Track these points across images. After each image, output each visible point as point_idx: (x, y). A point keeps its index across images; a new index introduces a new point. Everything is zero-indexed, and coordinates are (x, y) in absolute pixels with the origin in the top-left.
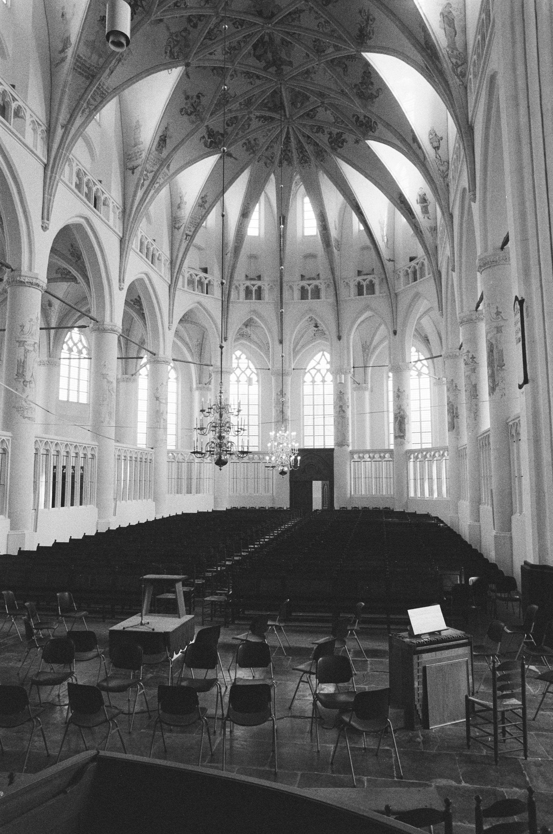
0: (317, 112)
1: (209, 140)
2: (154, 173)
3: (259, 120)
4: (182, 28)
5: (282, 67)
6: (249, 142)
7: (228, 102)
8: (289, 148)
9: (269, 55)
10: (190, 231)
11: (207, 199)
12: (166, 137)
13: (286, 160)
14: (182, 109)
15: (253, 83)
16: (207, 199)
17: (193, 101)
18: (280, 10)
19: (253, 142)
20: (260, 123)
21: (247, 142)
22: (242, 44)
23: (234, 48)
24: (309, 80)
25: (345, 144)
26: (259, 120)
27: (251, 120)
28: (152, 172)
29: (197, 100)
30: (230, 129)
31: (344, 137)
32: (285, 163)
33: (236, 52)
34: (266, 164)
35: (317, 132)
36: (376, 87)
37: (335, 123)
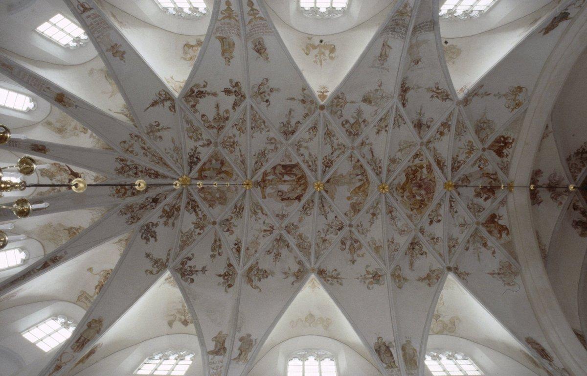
0: (191, 214)
1: (196, 91)
2: (247, 23)
3: (192, 150)
4: (344, 113)
5: (259, 187)
6: (159, 130)
7: (252, 129)
8: (140, 174)
9: (270, 177)
10: (89, 17)
11: (118, 58)
12: (261, 54)
13: (123, 168)
14: (267, 82)
15: (254, 157)
16: (118, 58)
17: (266, 94)
18: (333, 198)
19: (158, 134)
20: (189, 150)
21: (160, 127)
22: (302, 158)
23: (298, 150)
24: (250, 214)
25: (145, 241)
26: (192, 150)
27: (195, 140)
28: (250, 22)
29: (265, 100)
30: (198, 116)
31: (152, 240)
32: (119, 166)
33: (296, 150)
34: (124, 142)
35: (164, 211)
36: (258, 284)
37: (182, 233)
